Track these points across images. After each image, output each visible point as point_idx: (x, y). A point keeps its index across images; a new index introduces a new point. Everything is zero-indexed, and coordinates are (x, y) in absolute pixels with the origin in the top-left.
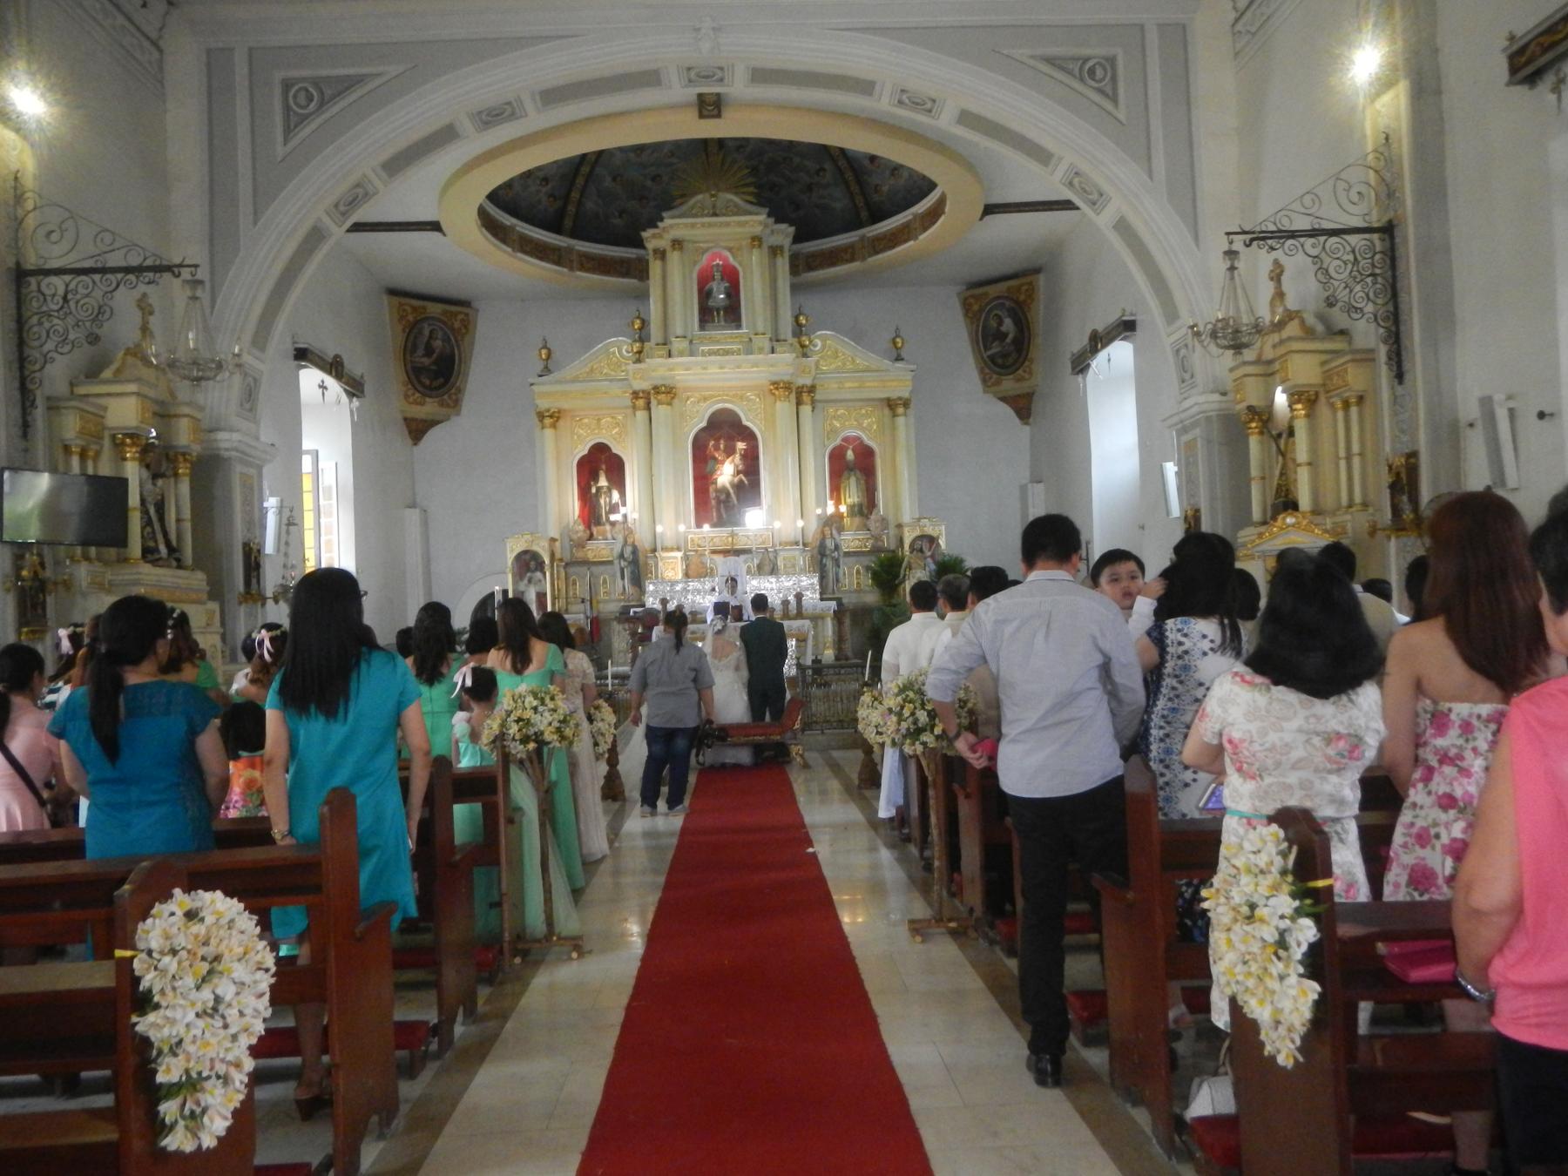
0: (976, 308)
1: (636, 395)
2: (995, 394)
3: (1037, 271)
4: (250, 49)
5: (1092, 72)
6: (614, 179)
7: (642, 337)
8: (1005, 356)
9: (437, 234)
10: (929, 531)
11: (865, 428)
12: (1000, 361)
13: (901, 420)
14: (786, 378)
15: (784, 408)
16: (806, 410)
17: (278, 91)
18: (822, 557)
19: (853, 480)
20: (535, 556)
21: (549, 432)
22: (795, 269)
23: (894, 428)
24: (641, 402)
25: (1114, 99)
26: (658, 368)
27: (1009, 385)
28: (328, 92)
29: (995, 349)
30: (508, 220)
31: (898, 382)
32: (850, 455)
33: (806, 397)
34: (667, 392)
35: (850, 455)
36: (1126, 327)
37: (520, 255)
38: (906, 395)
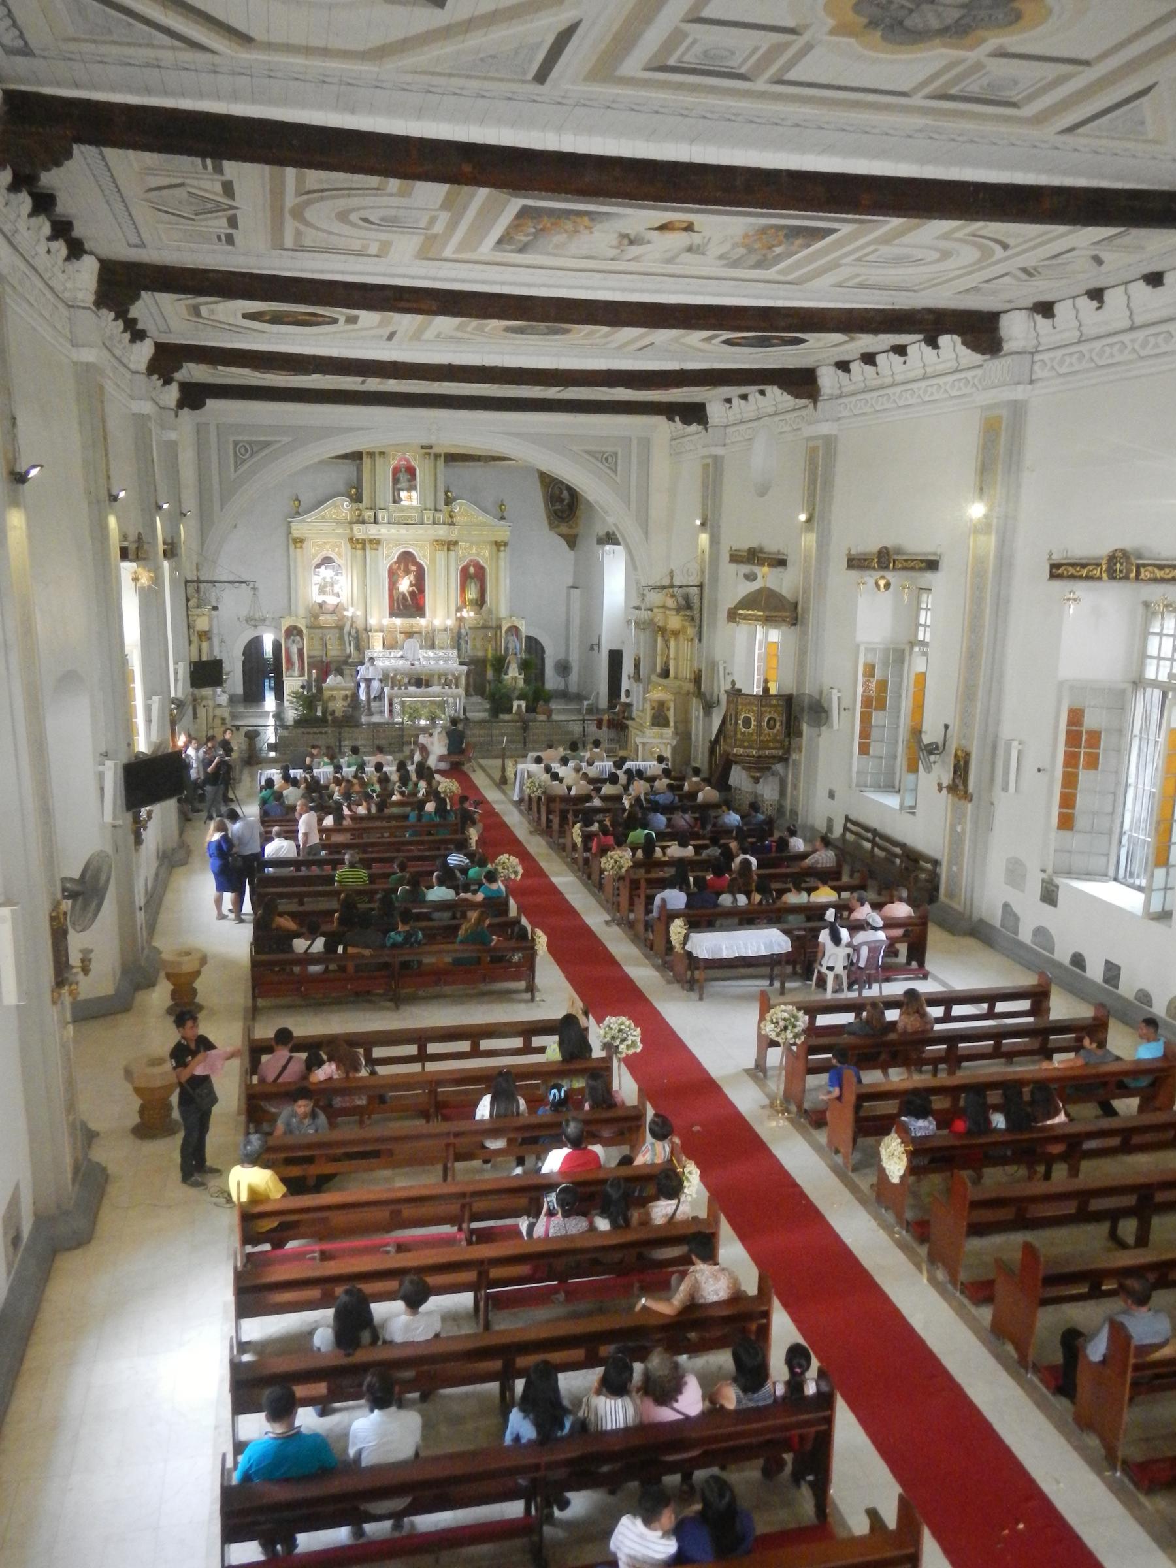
4: (217, 426)
5: (607, 459)
7: (357, 499)
8: (562, 511)
10: (516, 624)
11: (484, 556)
13: (502, 554)
15: (441, 555)
17: (231, 446)
18: (458, 641)
19: (473, 585)
20: (295, 628)
22: (445, 461)
23: (498, 558)
24: (359, 546)
25: (615, 471)
26: (373, 531)
27: (564, 529)
28: (255, 449)
29: (558, 506)
31: (502, 532)
32: (472, 570)
33: (452, 548)
34: (376, 542)
35: (472, 570)
38: (505, 539)
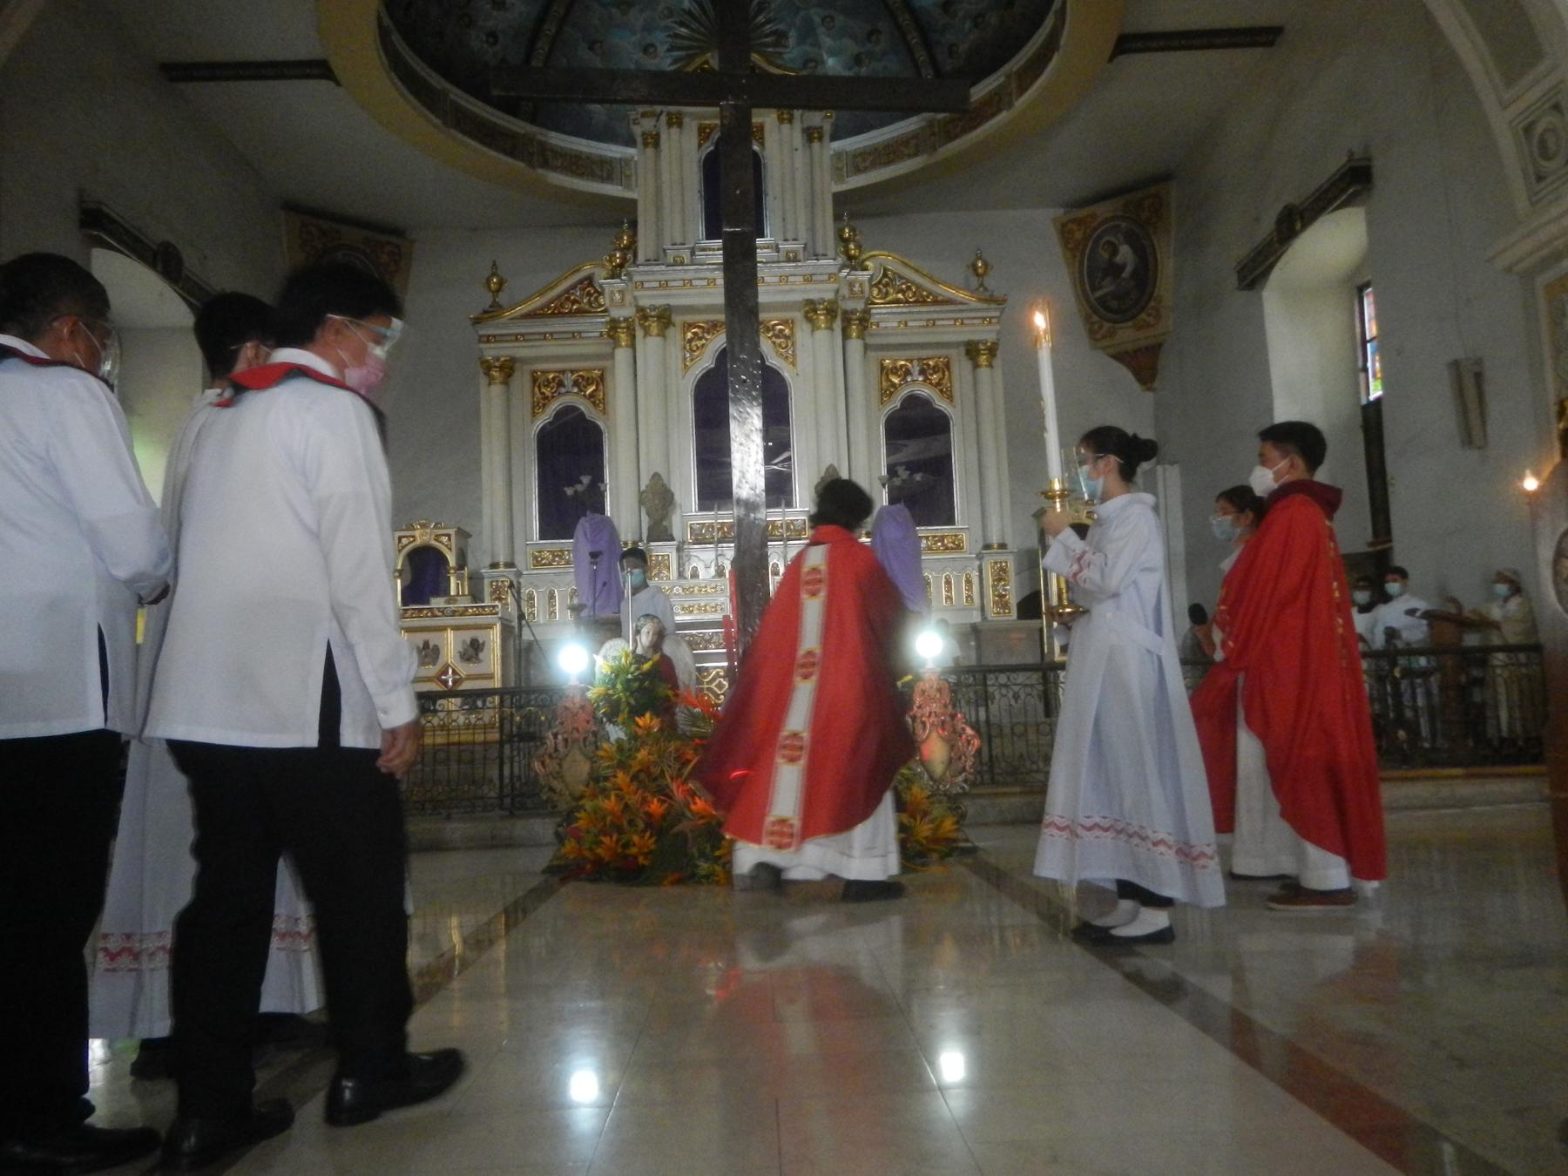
0: (1078, 235)
1: (614, 325)
2: (1103, 349)
3: (1165, 177)
6: (591, 48)
9: (324, 84)
12: (1114, 304)
13: (984, 372)
14: (830, 296)
16: (855, 345)
21: (497, 389)
27: (1127, 335)
29: (1108, 287)
30: (436, 81)
36: (1353, 182)
37: (453, 131)
38: (991, 337)
